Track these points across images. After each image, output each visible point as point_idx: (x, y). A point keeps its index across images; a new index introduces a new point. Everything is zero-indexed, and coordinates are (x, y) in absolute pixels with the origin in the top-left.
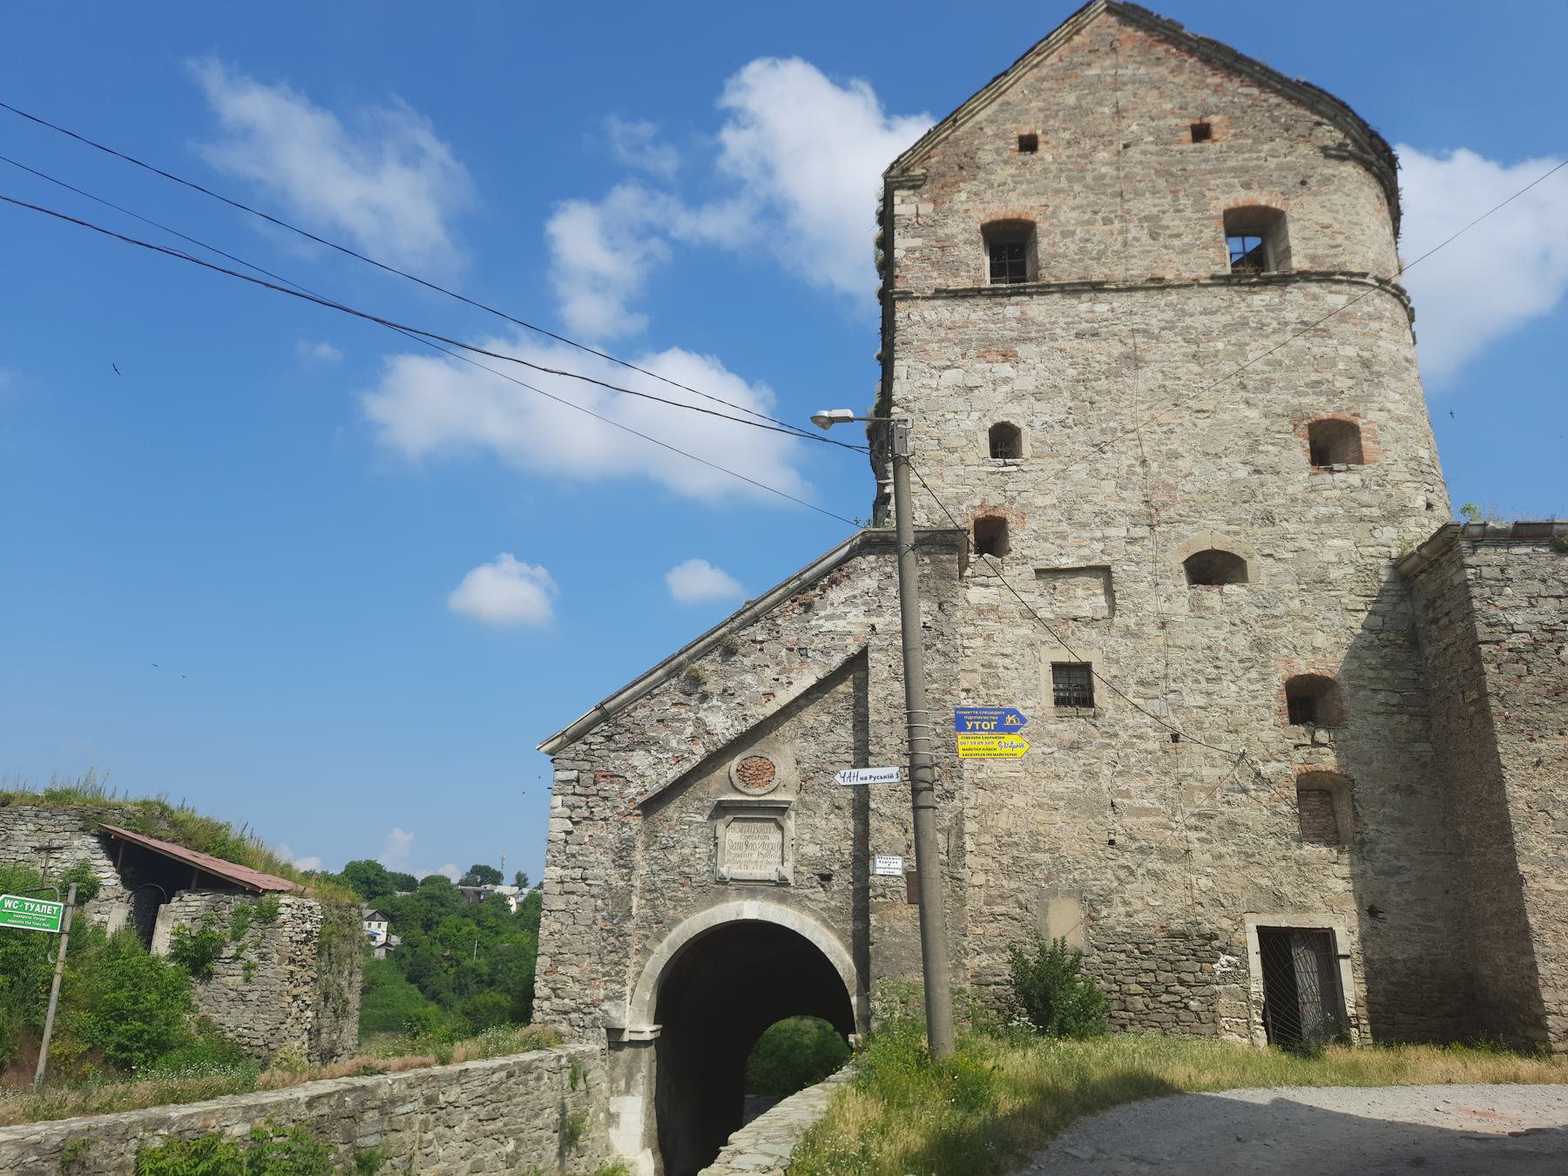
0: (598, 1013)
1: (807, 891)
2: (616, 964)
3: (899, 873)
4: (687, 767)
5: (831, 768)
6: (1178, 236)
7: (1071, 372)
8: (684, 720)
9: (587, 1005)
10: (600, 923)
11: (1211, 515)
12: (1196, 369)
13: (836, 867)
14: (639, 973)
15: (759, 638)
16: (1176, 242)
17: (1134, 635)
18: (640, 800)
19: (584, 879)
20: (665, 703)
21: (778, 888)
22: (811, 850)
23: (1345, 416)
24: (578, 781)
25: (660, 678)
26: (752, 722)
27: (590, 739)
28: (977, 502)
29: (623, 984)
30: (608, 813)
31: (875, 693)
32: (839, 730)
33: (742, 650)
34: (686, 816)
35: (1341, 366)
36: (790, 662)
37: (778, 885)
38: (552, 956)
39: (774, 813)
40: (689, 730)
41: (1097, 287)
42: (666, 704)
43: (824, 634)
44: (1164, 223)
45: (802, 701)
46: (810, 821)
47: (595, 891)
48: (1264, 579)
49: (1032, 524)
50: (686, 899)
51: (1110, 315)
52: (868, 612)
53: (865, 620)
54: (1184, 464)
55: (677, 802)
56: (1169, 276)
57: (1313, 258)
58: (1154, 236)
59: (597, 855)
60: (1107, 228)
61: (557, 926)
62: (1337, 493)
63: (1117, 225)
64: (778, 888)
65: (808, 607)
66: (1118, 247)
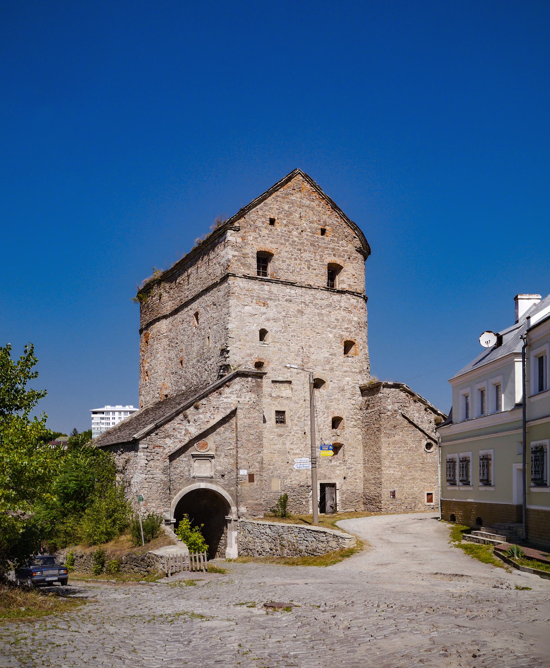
4: (183, 444)
6: (315, 269)
7: (284, 314)
11: (319, 367)
12: (318, 319)
16: (314, 272)
17: (298, 403)
23: (353, 340)
26: (203, 430)
28: (256, 356)
32: (227, 433)
34: (183, 458)
35: (353, 323)
40: (184, 432)
41: (292, 284)
43: (224, 403)
44: (311, 264)
48: (330, 388)
49: (272, 365)
51: (295, 295)
52: (237, 397)
53: (236, 399)
54: (312, 350)
56: (312, 284)
57: (349, 285)
58: (309, 268)
60: (296, 262)
62: (349, 364)
63: (298, 262)
66: (298, 270)
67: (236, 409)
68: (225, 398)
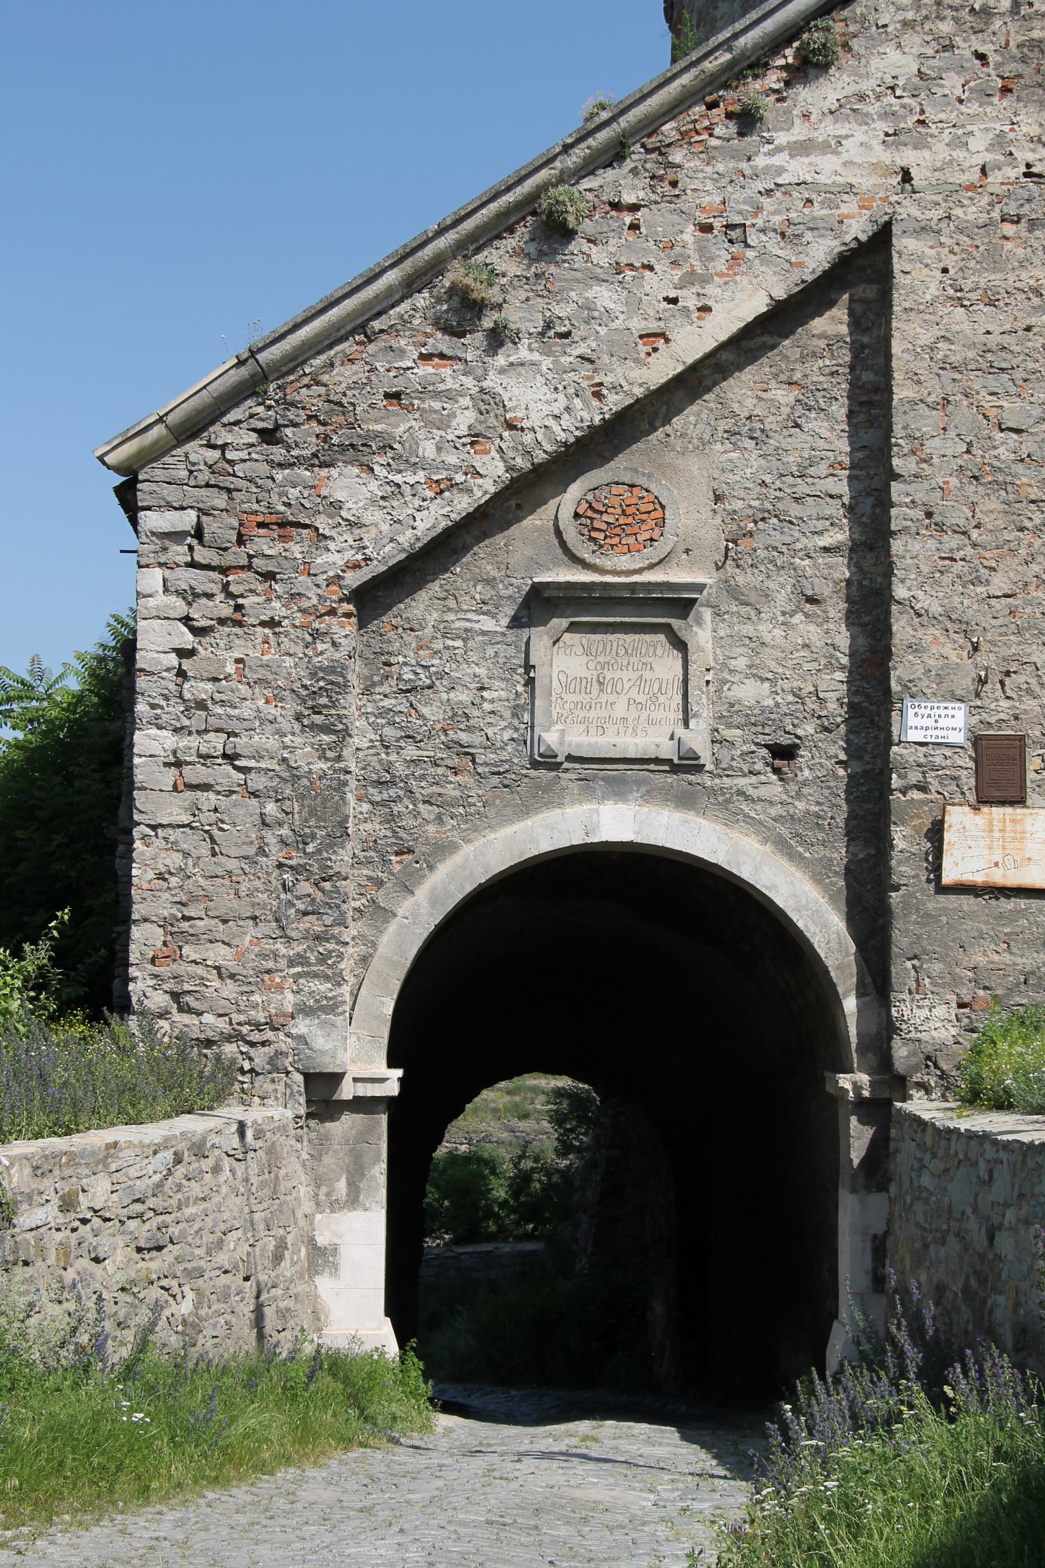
0: (282, 1042)
1: (741, 782)
2: (318, 938)
3: (958, 738)
4: (462, 505)
5: (795, 510)
8: (449, 396)
9: (258, 1026)
10: (276, 853)
13: (808, 729)
14: (365, 960)
15: (629, 198)
18: (353, 579)
19: (230, 758)
20: (402, 352)
21: (678, 772)
22: (749, 693)
24: (198, 533)
25: (390, 290)
26: (615, 402)
27: (220, 434)
29: (338, 980)
30: (277, 608)
31: (908, 337)
32: (814, 423)
33: (587, 226)
34: (460, 620)
36: (706, 257)
37: (676, 769)
38: (165, 923)
39: (665, 610)
40: (464, 419)
42: (406, 348)
45: (724, 356)
46: (748, 629)
47: (257, 782)
50: (464, 801)
52: (893, 138)
53: (885, 156)
55: (435, 588)
59: (252, 704)
61: (175, 860)
64: (678, 772)
65: (747, 120)
67: (882, 238)
68: (801, 148)
